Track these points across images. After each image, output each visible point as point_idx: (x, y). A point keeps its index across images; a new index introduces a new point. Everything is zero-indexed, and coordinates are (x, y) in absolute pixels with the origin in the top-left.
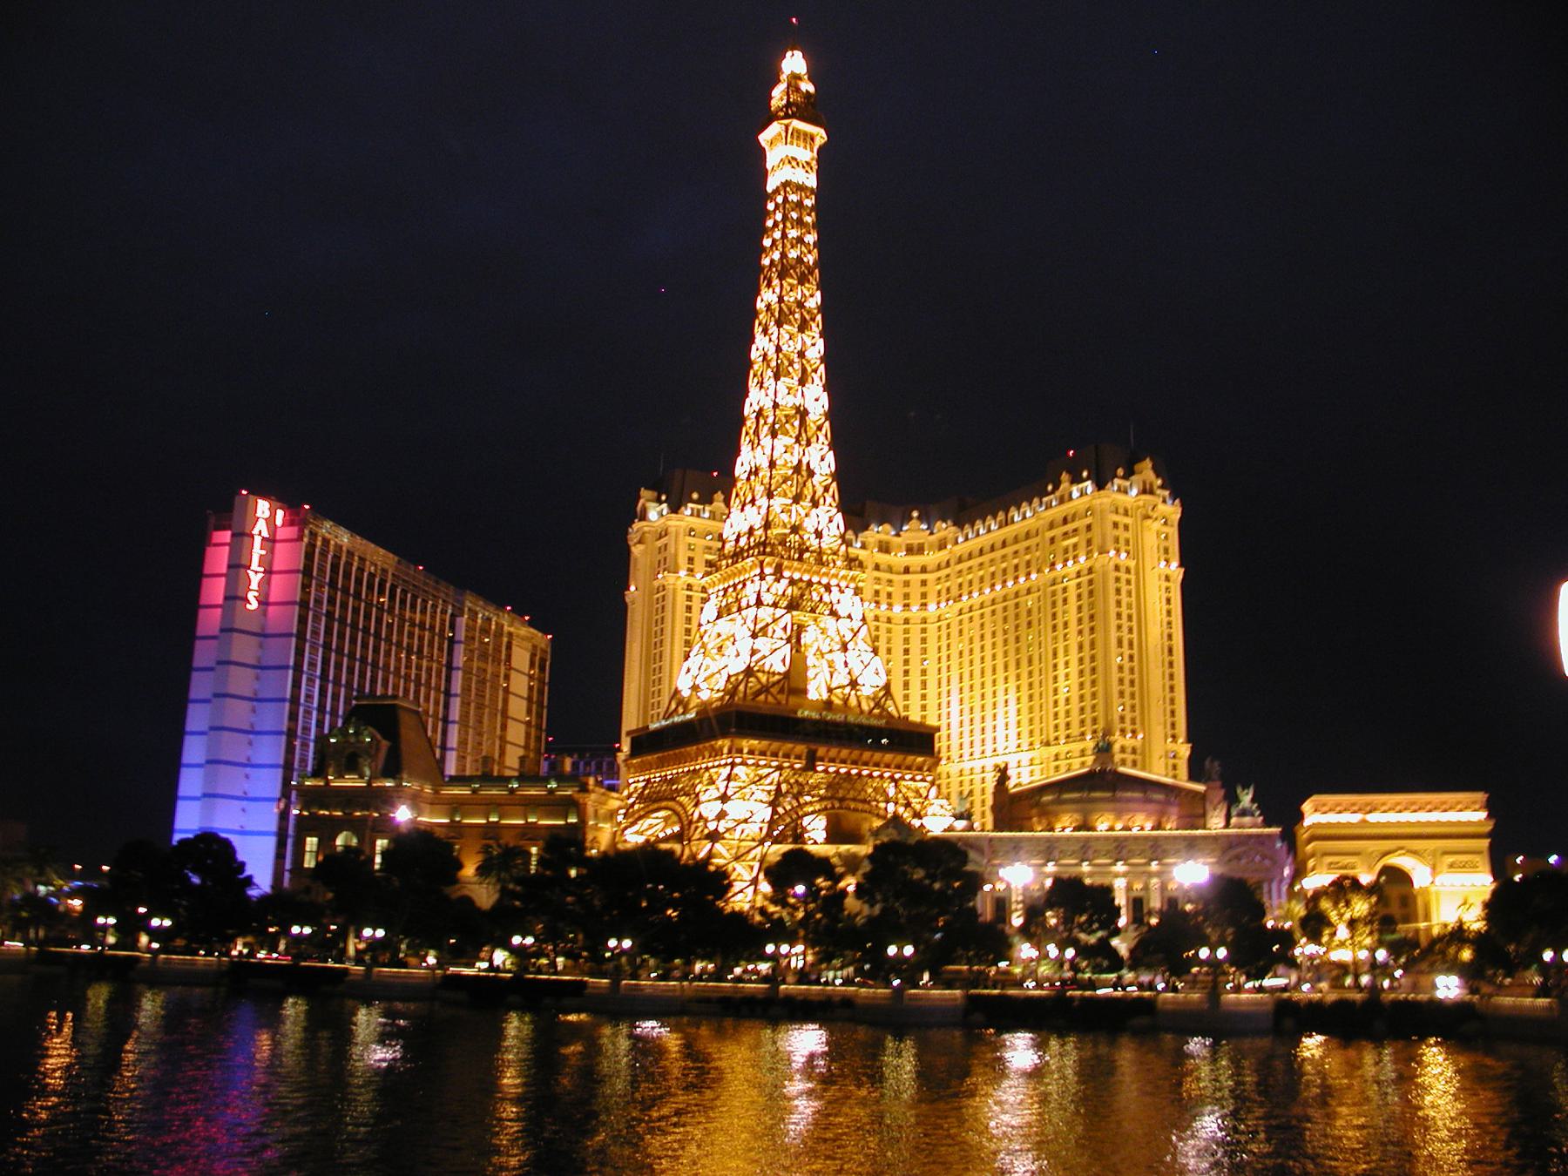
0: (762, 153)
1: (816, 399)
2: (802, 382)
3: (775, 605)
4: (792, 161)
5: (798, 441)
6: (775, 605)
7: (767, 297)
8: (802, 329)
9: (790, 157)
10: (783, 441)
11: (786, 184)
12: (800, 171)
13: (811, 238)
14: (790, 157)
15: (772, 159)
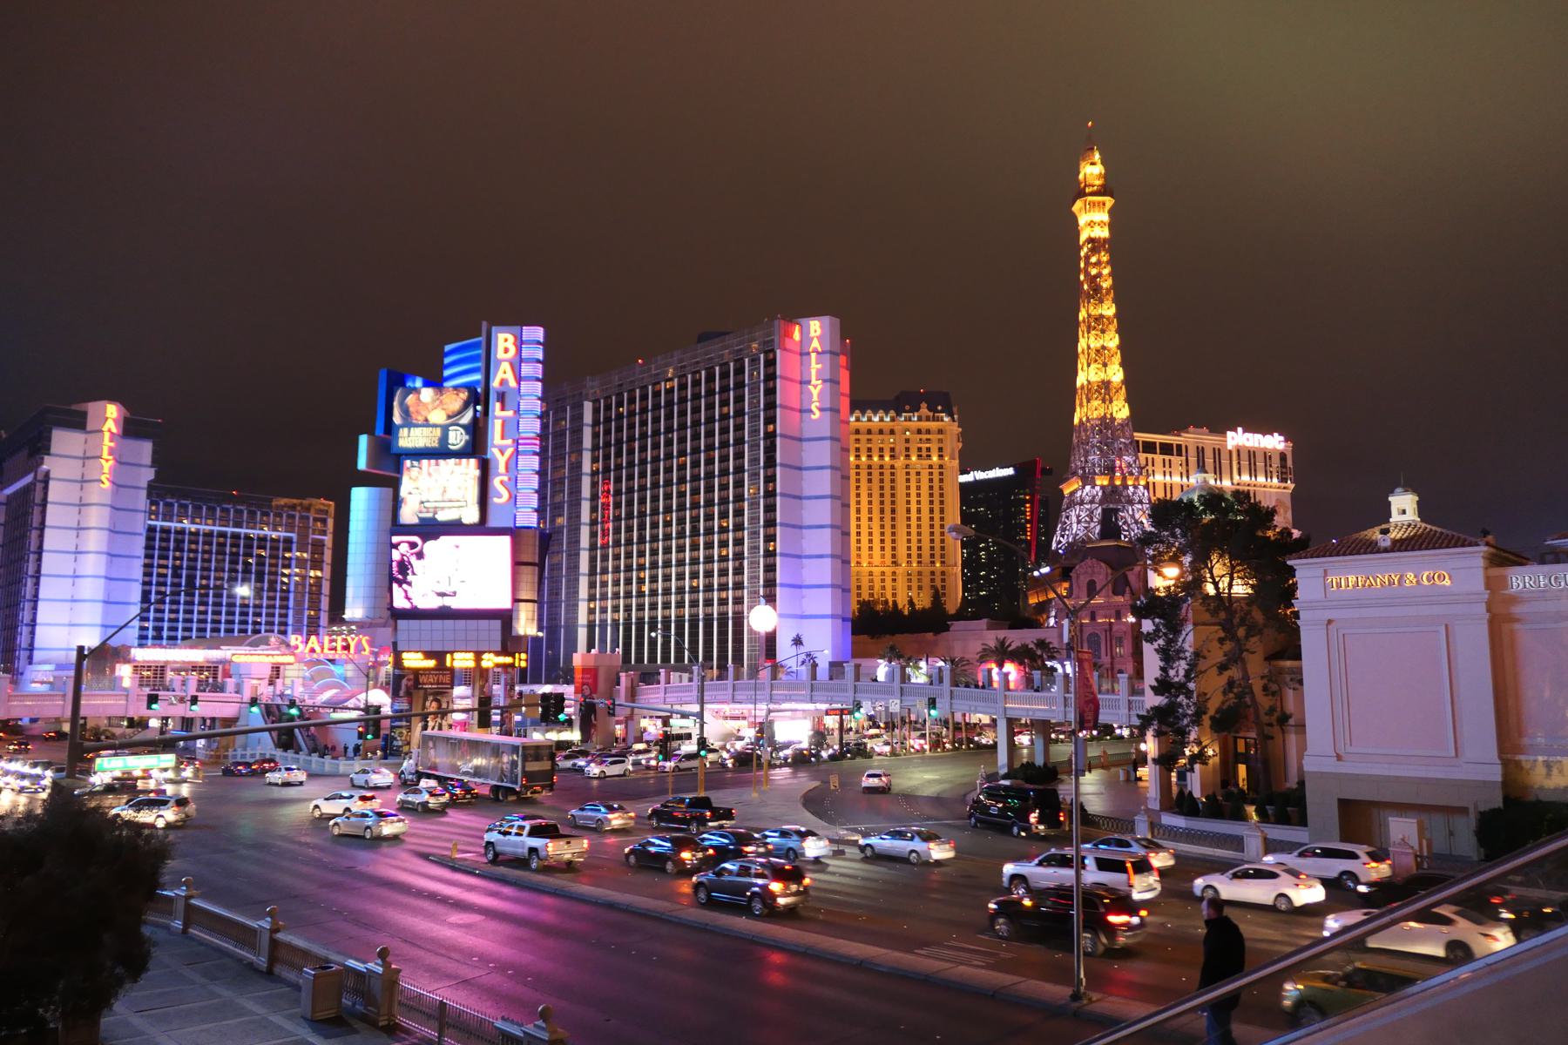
0: (1074, 219)
1: (1116, 374)
2: (1105, 365)
3: (1092, 502)
4: (1091, 224)
5: (1104, 401)
6: (1092, 502)
7: (1082, 314)
8: (1103, 331)
9: (1093, 221)
10: (1095, 403)
11: (1090, 240)
12: (1097, 228)
13: (1106, 271)
14: (1093, 221)
15: (1083, 220)
